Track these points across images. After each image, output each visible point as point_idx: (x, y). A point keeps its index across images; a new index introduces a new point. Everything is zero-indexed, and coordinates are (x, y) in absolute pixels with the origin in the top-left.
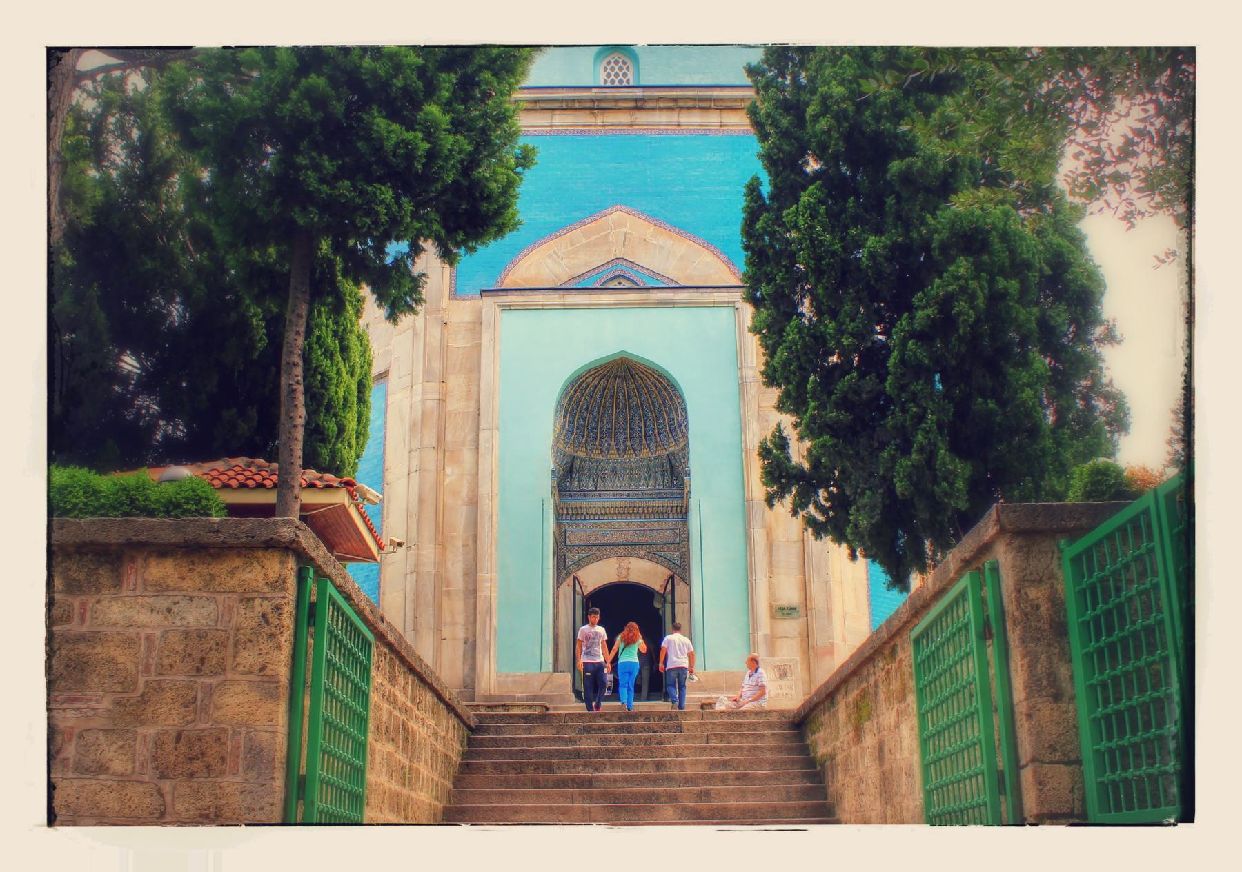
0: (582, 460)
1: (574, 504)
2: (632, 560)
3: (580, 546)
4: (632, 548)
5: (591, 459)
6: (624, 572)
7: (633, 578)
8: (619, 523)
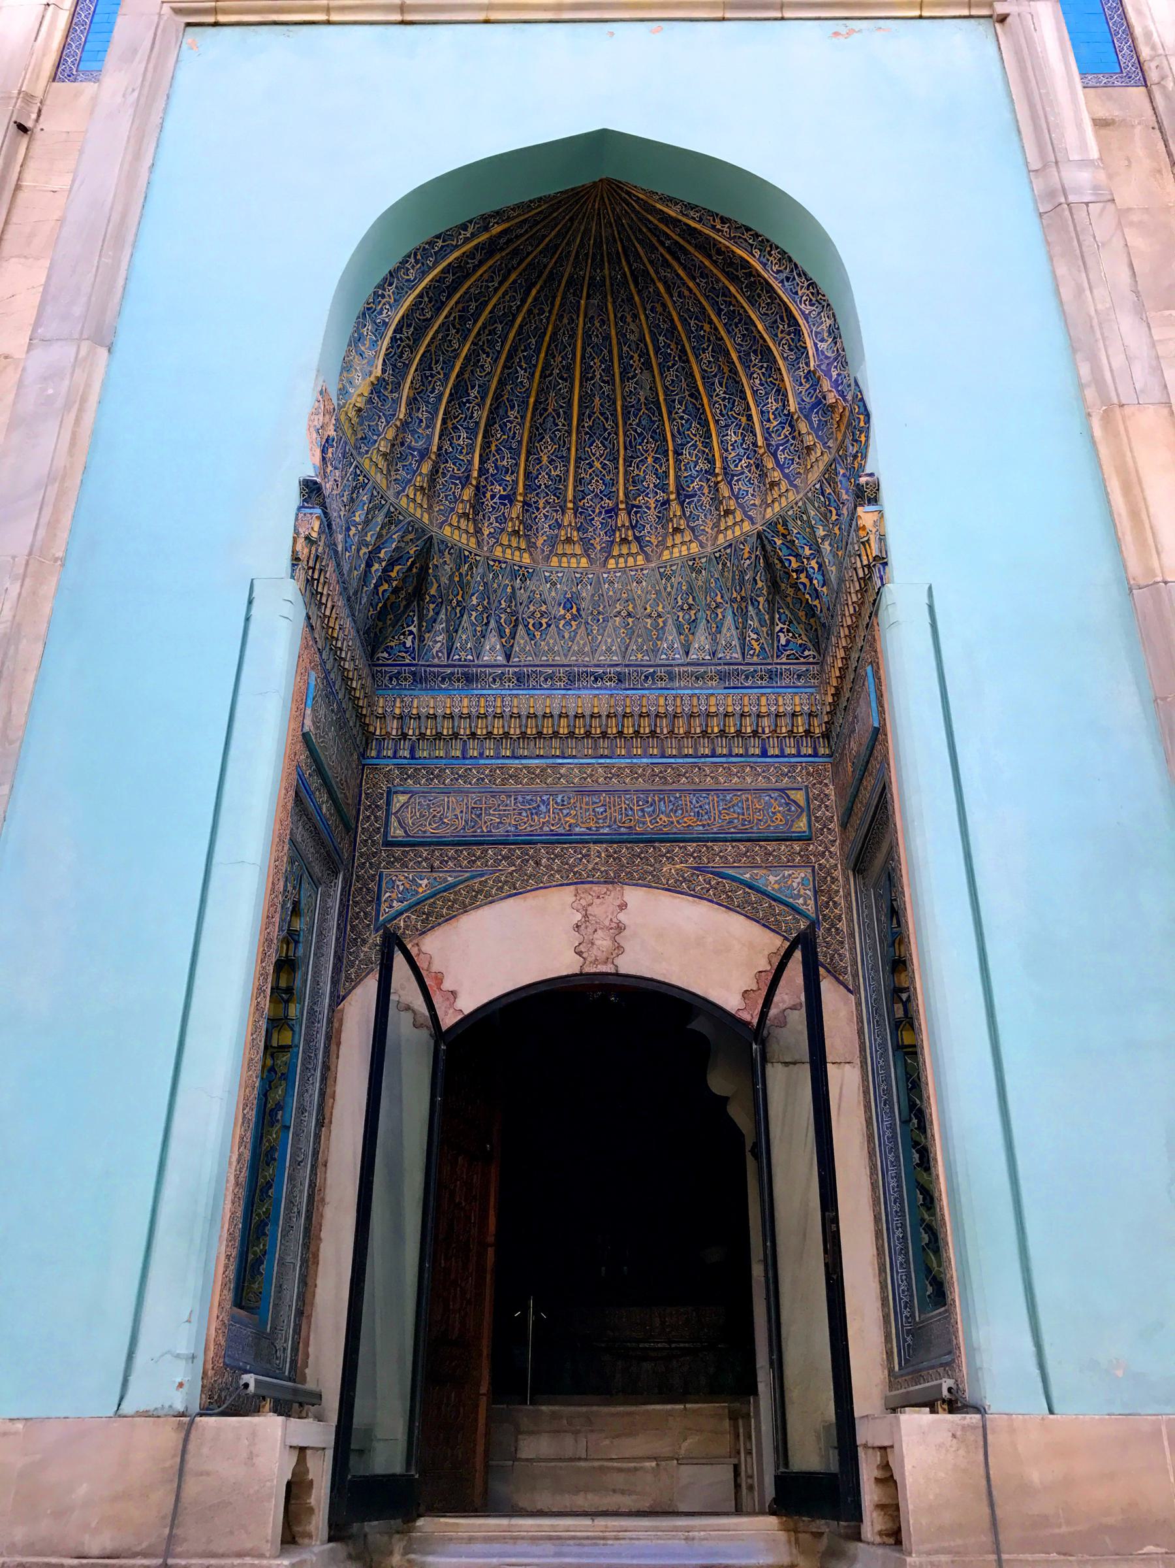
0: (461, 557)
1: (425, 702)
2: (634, 896)
4: (635, 853)
5: (493, 564)
6: (603, 942)
7: (637, 961)
8: (577, 765)
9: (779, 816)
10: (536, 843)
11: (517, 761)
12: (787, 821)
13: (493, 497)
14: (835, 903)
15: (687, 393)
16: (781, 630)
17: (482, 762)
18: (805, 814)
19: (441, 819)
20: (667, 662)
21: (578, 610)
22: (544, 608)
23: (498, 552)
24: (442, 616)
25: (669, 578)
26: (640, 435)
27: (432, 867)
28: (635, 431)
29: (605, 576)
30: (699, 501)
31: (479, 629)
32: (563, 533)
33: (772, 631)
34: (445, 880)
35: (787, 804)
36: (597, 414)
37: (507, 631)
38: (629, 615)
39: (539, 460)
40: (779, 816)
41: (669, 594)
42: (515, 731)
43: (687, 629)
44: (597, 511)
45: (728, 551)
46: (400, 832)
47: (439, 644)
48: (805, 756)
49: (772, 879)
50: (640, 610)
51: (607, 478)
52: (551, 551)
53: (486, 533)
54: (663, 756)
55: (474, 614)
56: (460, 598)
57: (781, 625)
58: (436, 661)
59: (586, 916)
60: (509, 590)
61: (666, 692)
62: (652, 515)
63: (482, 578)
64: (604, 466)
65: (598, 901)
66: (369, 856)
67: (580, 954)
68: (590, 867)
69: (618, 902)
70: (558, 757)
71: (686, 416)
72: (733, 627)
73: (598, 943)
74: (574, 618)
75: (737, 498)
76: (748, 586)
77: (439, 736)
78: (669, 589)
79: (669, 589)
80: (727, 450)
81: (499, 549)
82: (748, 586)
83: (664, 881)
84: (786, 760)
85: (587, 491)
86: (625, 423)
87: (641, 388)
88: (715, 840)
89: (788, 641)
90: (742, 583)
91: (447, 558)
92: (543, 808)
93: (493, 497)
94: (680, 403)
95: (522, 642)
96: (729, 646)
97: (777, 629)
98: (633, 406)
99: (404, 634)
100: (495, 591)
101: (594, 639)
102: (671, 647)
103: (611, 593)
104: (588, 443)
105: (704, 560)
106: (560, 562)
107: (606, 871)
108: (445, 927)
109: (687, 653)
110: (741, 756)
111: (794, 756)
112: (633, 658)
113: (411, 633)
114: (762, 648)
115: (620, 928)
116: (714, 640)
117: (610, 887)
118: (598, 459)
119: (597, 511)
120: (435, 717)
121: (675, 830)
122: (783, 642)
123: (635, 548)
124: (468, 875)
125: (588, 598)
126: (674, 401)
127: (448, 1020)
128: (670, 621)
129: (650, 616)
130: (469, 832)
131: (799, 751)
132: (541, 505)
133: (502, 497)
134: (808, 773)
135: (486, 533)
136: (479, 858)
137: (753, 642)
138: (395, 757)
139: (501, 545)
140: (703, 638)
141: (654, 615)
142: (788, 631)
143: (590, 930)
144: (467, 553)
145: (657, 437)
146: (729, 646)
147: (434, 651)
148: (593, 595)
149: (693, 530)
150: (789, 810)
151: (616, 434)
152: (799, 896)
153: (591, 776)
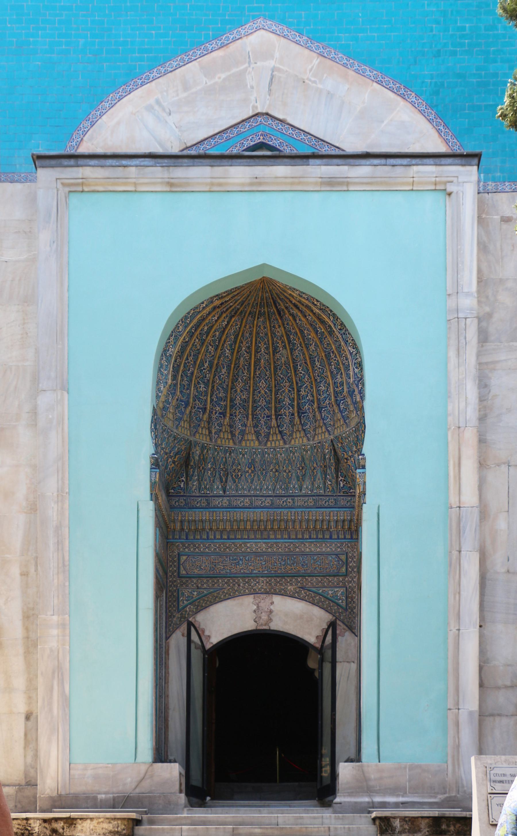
0: (203, 448)
2: (277, 599)
3: (200, 577)
9: (335, 566)
10: (238, 577)
11: (229, 541)
12: (338, 568)
13: (216, 413)
14: (354, 602)
15: (303, 361)
16: (341, 480)
17: (215, 541)
18: (345, 565)
19: (200, 567)
20: (292, 494)
21: (254, 468)
22: (239, 467)
23: (219, 442)
24: (196, 473)
25: (294, 454)
26: (282, 378)
27: (198, 586)
28: (280, 377)
29: (266, 450)
30: (308, 415)
31: (212, 479)
32: (247, 429)
33: (337, 481)
34: (203, 592)
35: (338, 561)
36: (263, 368)
37: (224, 479)
38: (277, 471)
39: (236, 391)
40: (335, 566)
41: (294, 461)
42: (228, 528)
43: (301, 479)
44: (263, 416)
45: (319, 445)
46: (184, 572)
47: (195, 486)
48: (347, 539)
49: (330, 592)
50: (281, 468)
51: (267, 399)
52: (242, 438)
53: (213, 432)
54: (290, 539)
55: (209, 472)
56: (203, 466)
57: (341, 478)
58: (194, 494)
59: (258, 607)
60: (224, 460)
61: (291, 510)
62: (287, 419)
63: (213, 455)
64: (266, 393)
65: (263, 601)
66: (173, 582)
67: (255, 622)
68: (260, 587)
69: (270, 602)
70: (246, 539)
71: (303, 372)
72: (320, 478)
73: (263, 617)
74: (252, 472)
75: (323, 420)
76: (328, 461)
77: (196, 530)
78: (294, 459)
79: (294, 459)
80: (320, 395)
81: (219, 440)
82: (328, 461)
83: (288, 593)
84: (340, 541)
85: (258, 406)
86: (275, 374)
87: (283, 356)
88: (309, 576)
89: (344, 485)
90: (325, 458)
91: (198, 448)
92: (241, 562)
93: (216, 413)
94: (300, 366)
95: (230, 484)
96: (319, 487)
97: (340, 479)
98: (279, 365)
99: (180, 481)
100: (218, 460)
101: (261, 483)
102: (294, 487)
103: (269, 459)
104: (258, 382)
105: (309, 447)
106: (246, 443)
107: (266, 589)
108: (204, 611)
109: (301, 490)
110: (321, 539)
111: (343, 539)
112: (278, 492)
113: (183, 481)
114: (333, 488)
115: (271, 612)
116: (313, 484)
117: (267, 595)
118: (263, 389)
119: (263, 416)
120: (195, 521)
121: (293, 572)
122: (342, 485)
123: (279, 437)
124: (212, 590)
125: (259, 462)
126: (297, 365)
127: (208, 646)
128: (294, 474)
129: (285, 471)
130: (212, 572)
131: (345, 537)
132: (237, 414)
133: (220, 413)
134: (348, 547)
135: (213, 432)
136: (216, 583)
137: (329, 486)
138: (180, 539)
139: (220, 438)
140: (308, 483)
141: (287, 471)
142: (344, 481)
143: (260, 612)
144: (206, 445)
145: (290, 380)
146: (319, 487)
147: (193, 489)
148: (261, 460)
149: (304, 430)
150: (339, 563)
151: (271, 378)
152: (340, 599)
153: (260, 547)
